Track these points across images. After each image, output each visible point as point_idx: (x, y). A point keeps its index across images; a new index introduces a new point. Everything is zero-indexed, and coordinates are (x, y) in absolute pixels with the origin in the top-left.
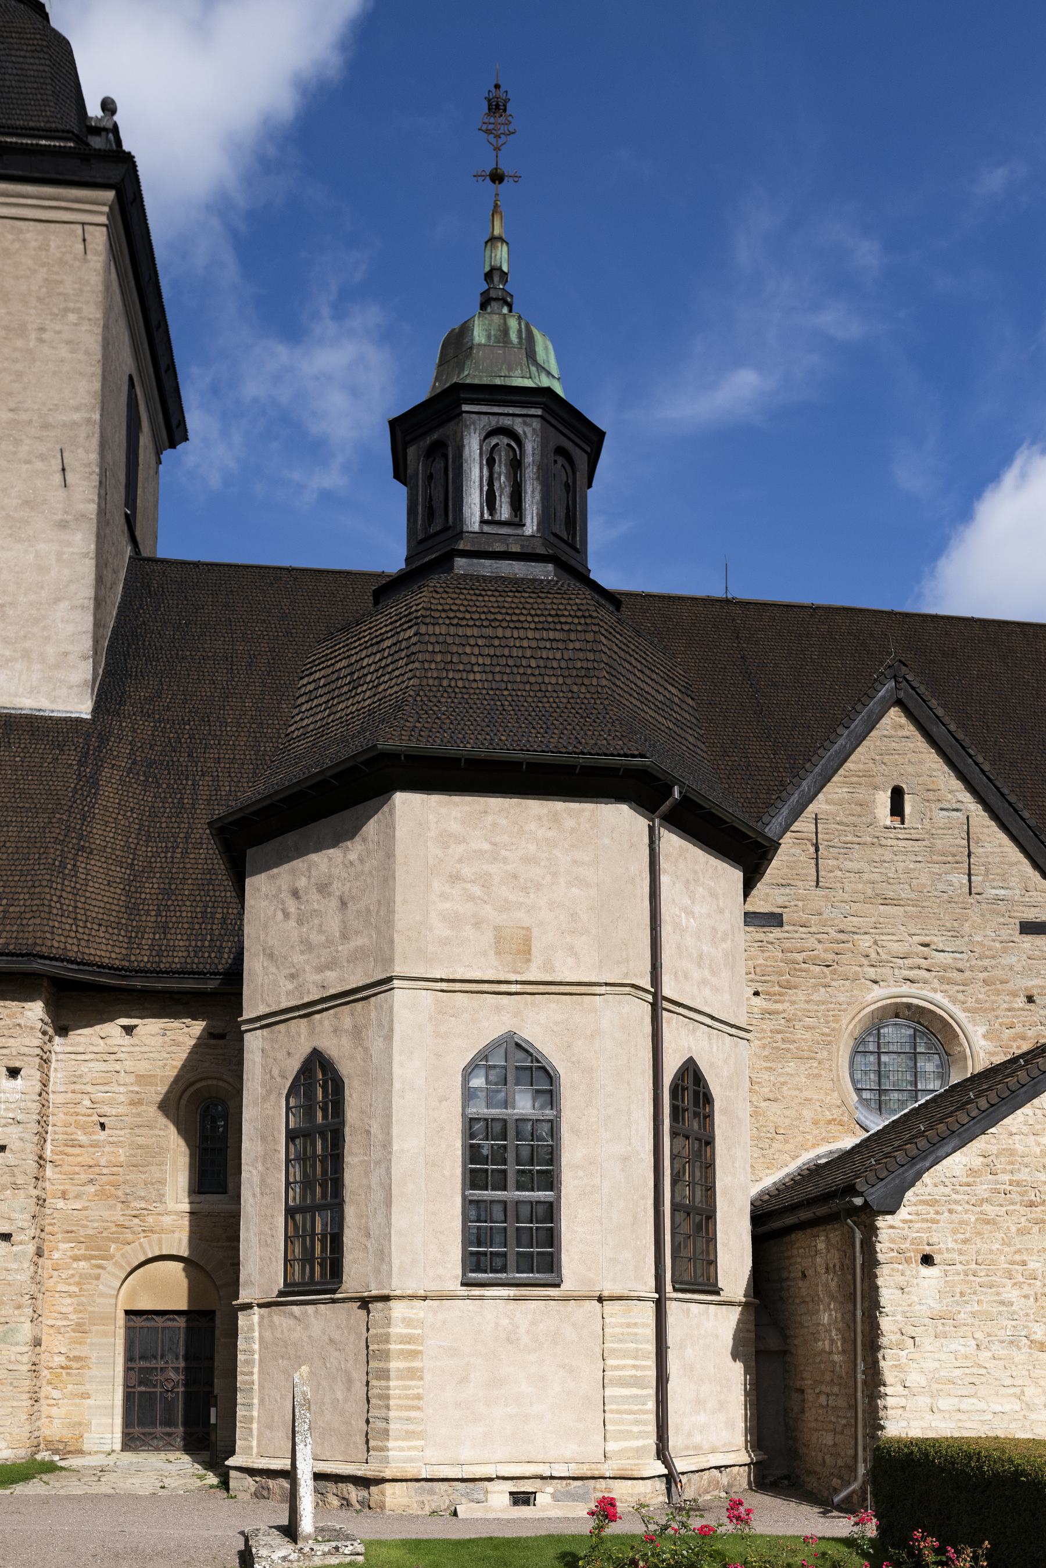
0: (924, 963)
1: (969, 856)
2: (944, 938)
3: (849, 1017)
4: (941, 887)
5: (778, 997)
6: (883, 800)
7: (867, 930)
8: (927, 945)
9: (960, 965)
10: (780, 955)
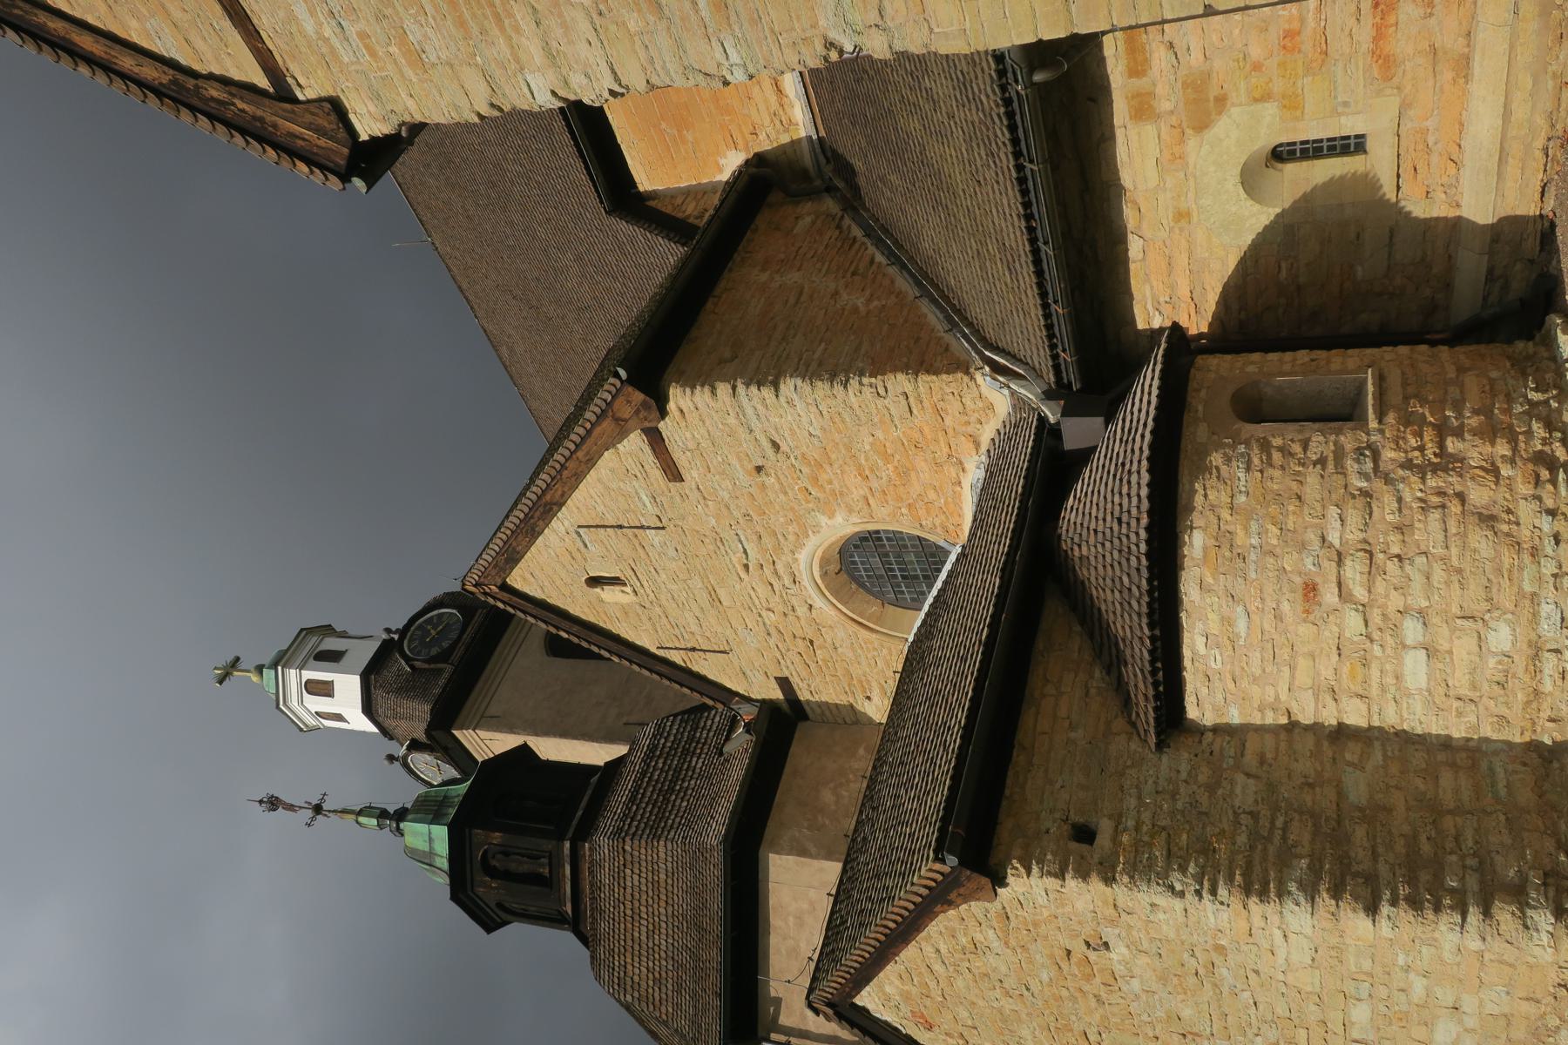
0: (768, 571)
1: (621, 527)
2: (729, 551)
3: (863, 633)
4: (672, 553)
5: (864, 684)
6: (609, 594)
7: (757, 616)
8: (746, 567)
9: (755, 538)
10: (818, 679)
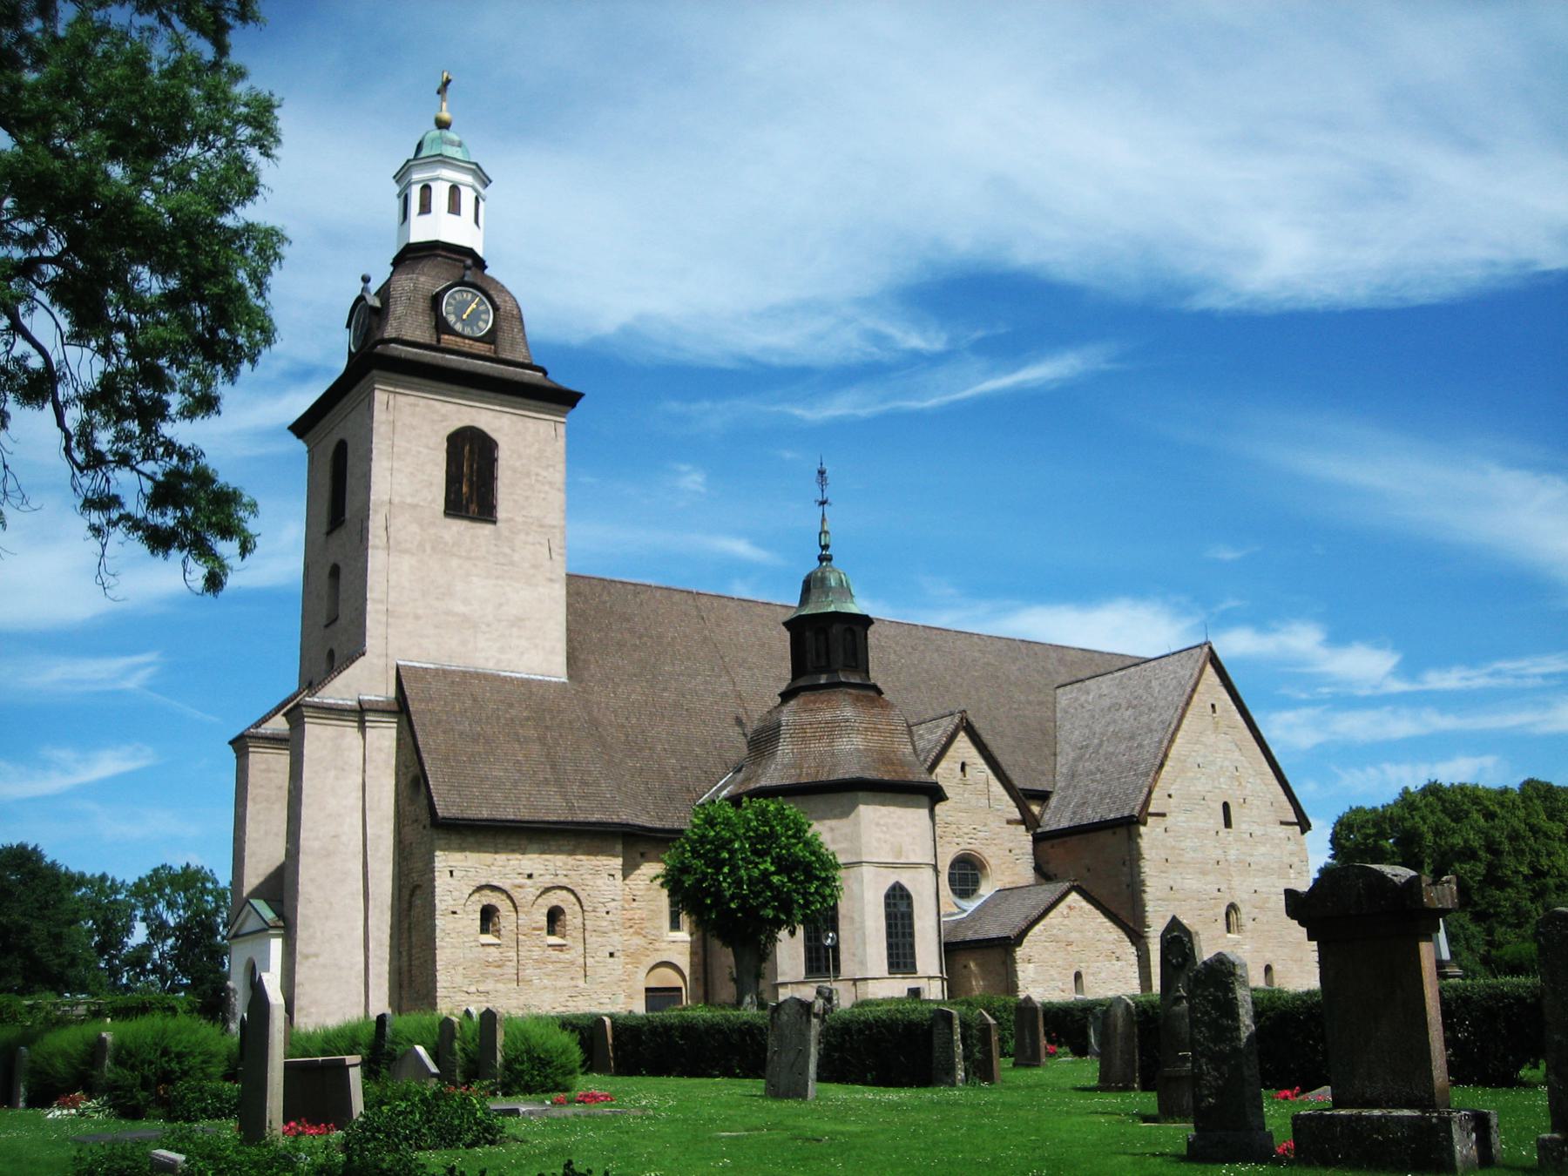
6: (959, 766)
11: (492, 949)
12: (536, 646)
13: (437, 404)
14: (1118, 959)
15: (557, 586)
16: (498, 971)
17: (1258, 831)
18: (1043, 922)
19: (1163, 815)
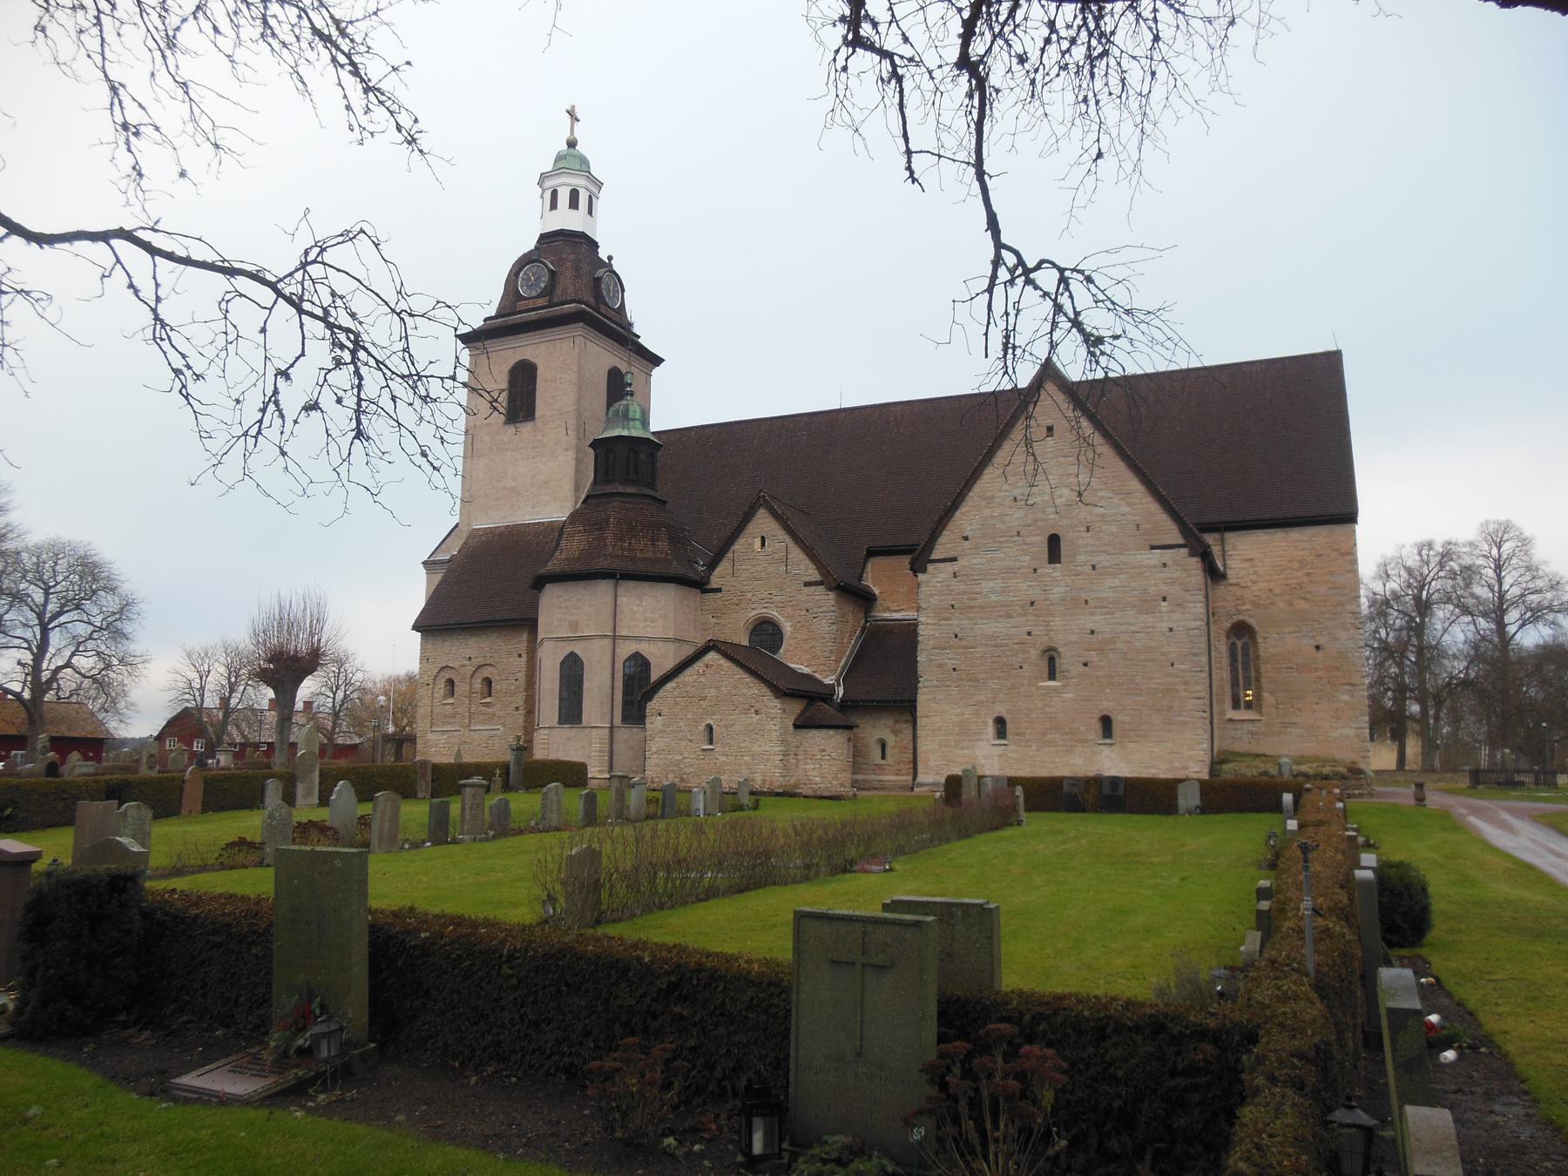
6: (758, 542)
11: (449, 706)
12: (555, 498)
13: (503, 353)
14: (757, 712)
15: (571, 453)
16: (452, 720)
17: (1103, 560)
18: (677, 680)
19: (954, 559)
